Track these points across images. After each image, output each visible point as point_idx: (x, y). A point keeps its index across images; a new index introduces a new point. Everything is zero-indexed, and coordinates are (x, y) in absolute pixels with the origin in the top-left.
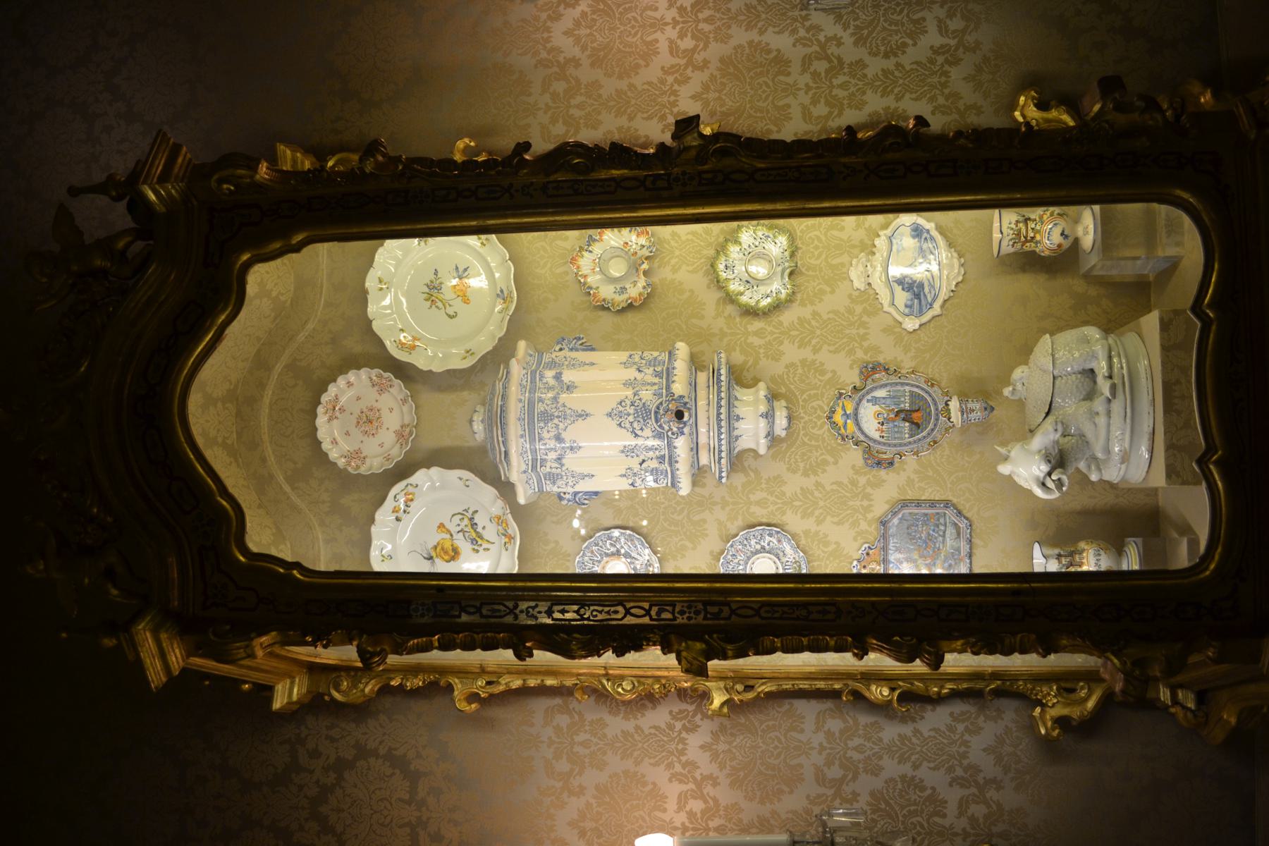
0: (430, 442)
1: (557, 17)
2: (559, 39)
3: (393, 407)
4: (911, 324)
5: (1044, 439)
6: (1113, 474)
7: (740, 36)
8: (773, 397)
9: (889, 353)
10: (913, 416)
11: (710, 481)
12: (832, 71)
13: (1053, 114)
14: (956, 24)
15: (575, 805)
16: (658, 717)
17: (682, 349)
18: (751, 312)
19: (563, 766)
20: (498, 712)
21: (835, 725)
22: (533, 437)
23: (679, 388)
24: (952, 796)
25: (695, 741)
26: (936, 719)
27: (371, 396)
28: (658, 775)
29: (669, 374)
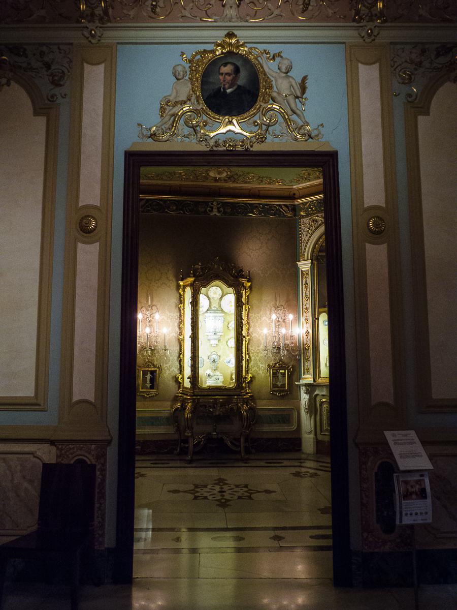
0: (212, 301)
1: (267, 318)
2: (264, 318)
3: (218, 296)
4: (225, 361)
5: (212, 374)
6: (207, 382)
7: (262, 342)
8: (217, 345)
9: (221, 359)
10: (214, 361)
11: (207, 337)
12: (257, 353)
13: (249, 379)
14: (262, 368)
15: (166, 318)
16: (177, 329)
17: (223, 334)
18: (227, 342)
19: (171, 317)
20: (177, 309)
21: (176, 351)
22: (213, 316)
23: (218, 334)
24: (168, 365)
25: (174, 334)
26: (177, 364)
27: (218, 293)
28: (170, 329)
29: (219, 332)
